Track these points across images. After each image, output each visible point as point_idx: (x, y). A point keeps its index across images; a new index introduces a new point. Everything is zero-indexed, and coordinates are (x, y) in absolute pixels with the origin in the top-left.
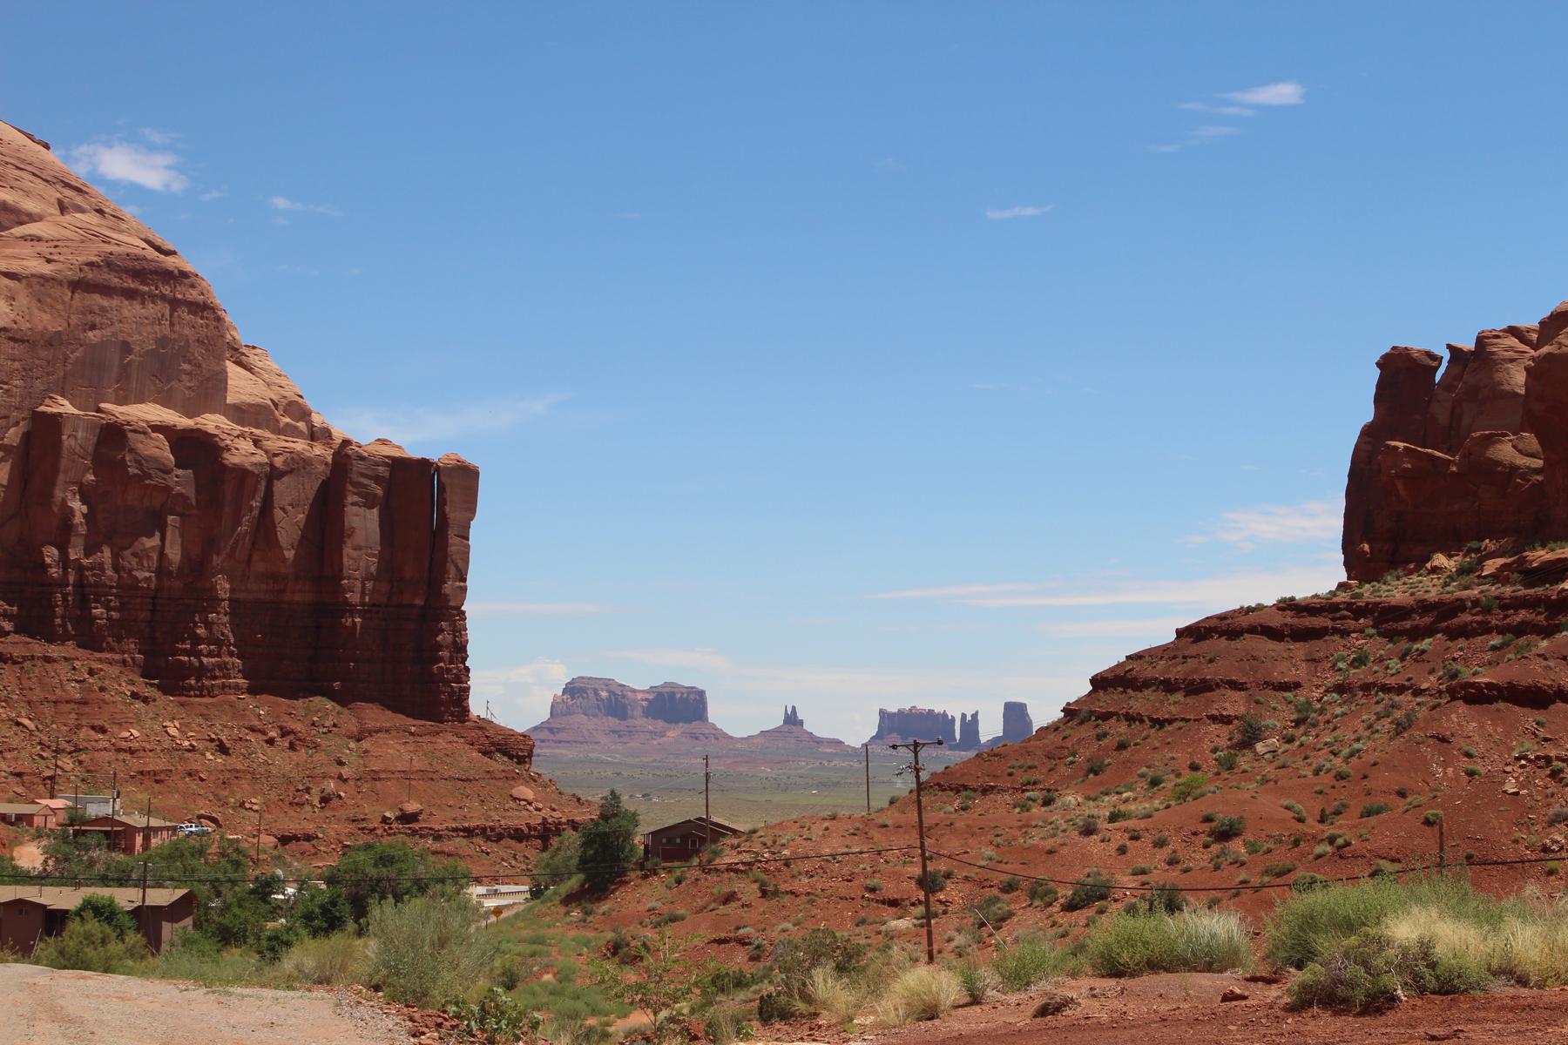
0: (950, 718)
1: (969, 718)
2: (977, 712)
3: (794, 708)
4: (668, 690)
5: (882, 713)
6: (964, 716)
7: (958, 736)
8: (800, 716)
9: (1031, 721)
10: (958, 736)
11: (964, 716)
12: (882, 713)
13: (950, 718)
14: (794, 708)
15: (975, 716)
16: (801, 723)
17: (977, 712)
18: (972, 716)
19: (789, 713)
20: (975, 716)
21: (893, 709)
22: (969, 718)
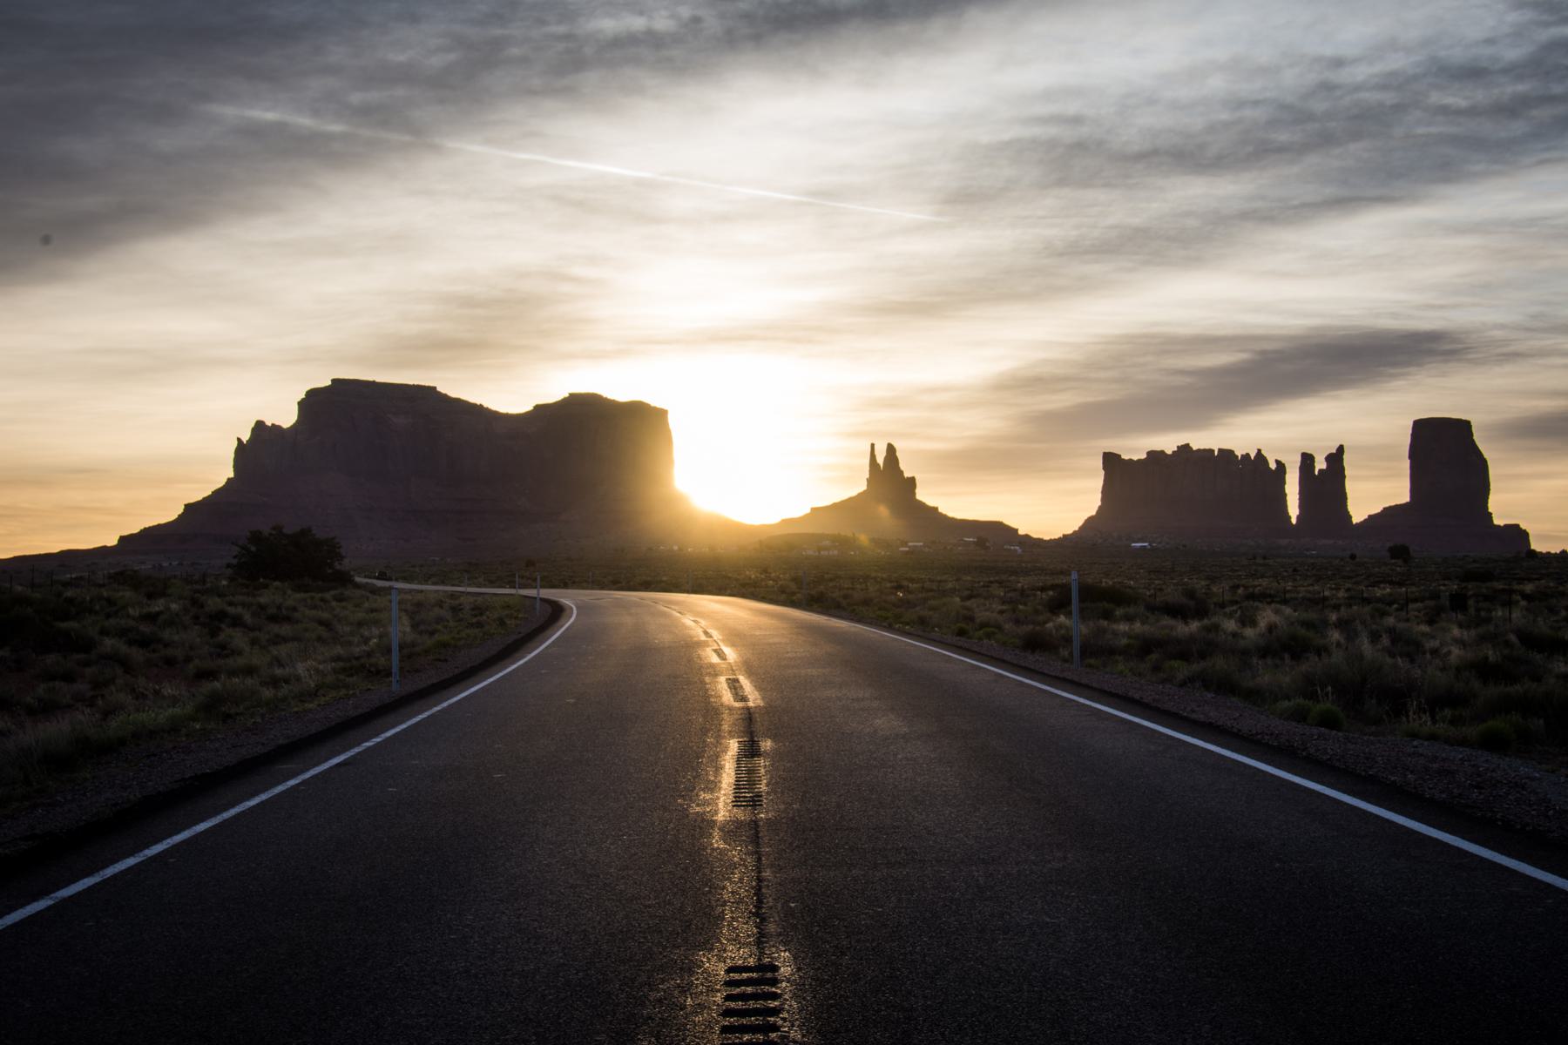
0: (1273, 466)
1: (1320, 465)
2: (1341, 449)
3: (891, 450)
7: (1293, 510)
10: (1293, 510)
11: (1307, 459)
12: (1111, 461)
13: (1273, 466)
14: (891, 450)
15: (1336, 459)
17: (1341, 449)
18: (1329, 458)
19: (880, 460)
20: (1336, 459)
22: (1320, 465)
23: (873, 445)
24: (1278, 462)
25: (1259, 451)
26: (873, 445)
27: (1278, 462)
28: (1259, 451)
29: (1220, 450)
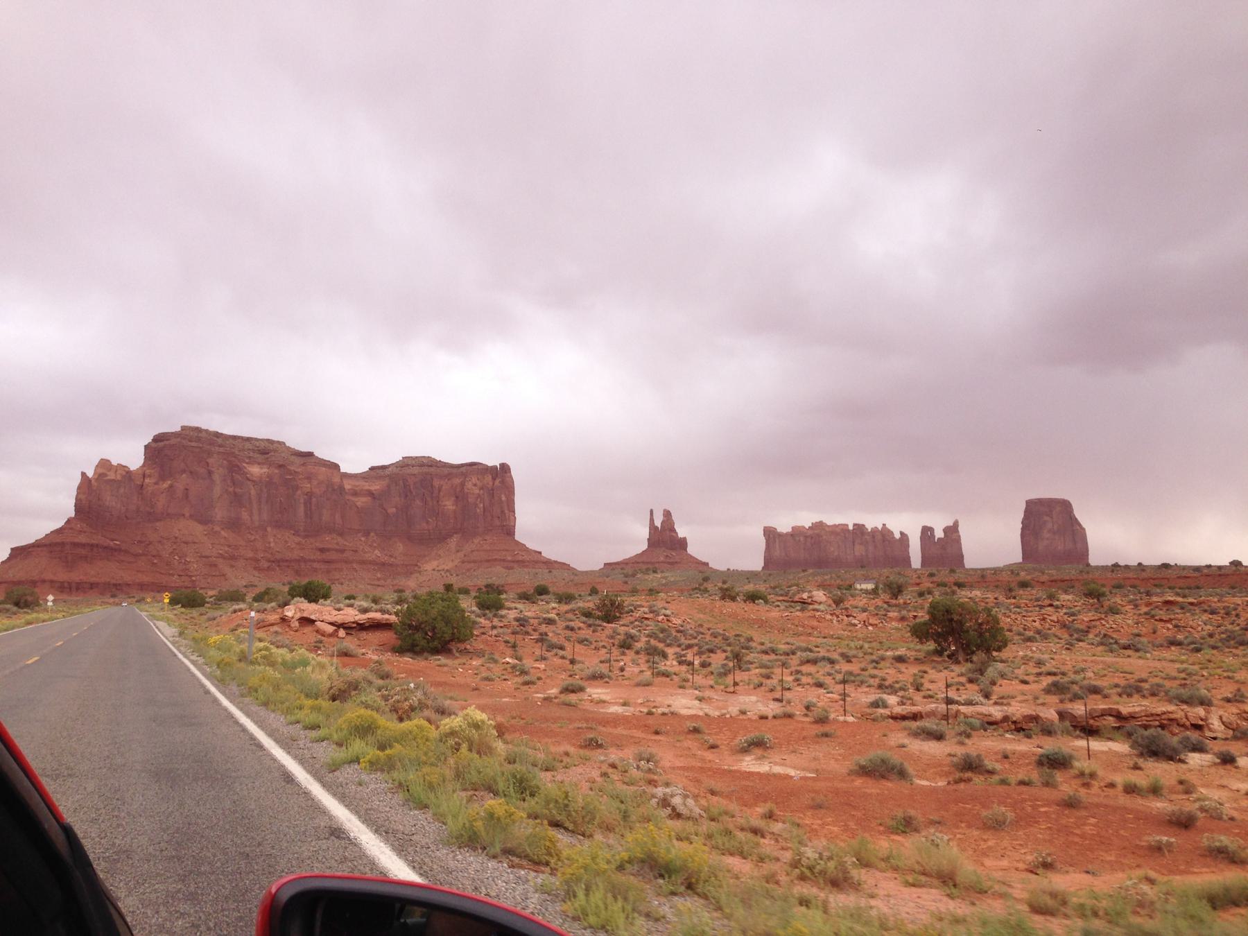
0: (897, 536)
1: (939, 534)
2: (956, 524)
3: (667, 514)
4: (416, 470)
5: (770, 533)
6: (927, 532)
8: (681, 532)
9: (1084, 529)
11: (927, 532)
12: (770, 533)
13: (897, 536)
14: (667, 514)
15: (952, 531)
16: (683, 543)
17: (956, 524)
19: (658, 523)
20: (952, 531)
21: (784, 525)
22: (939, 534)
23: (652, 512)
24: (902, 533)
25: (884, 525)
26: (652, 512)
27: (902, 533)
28: (884, 525)
29: (855, 525)
